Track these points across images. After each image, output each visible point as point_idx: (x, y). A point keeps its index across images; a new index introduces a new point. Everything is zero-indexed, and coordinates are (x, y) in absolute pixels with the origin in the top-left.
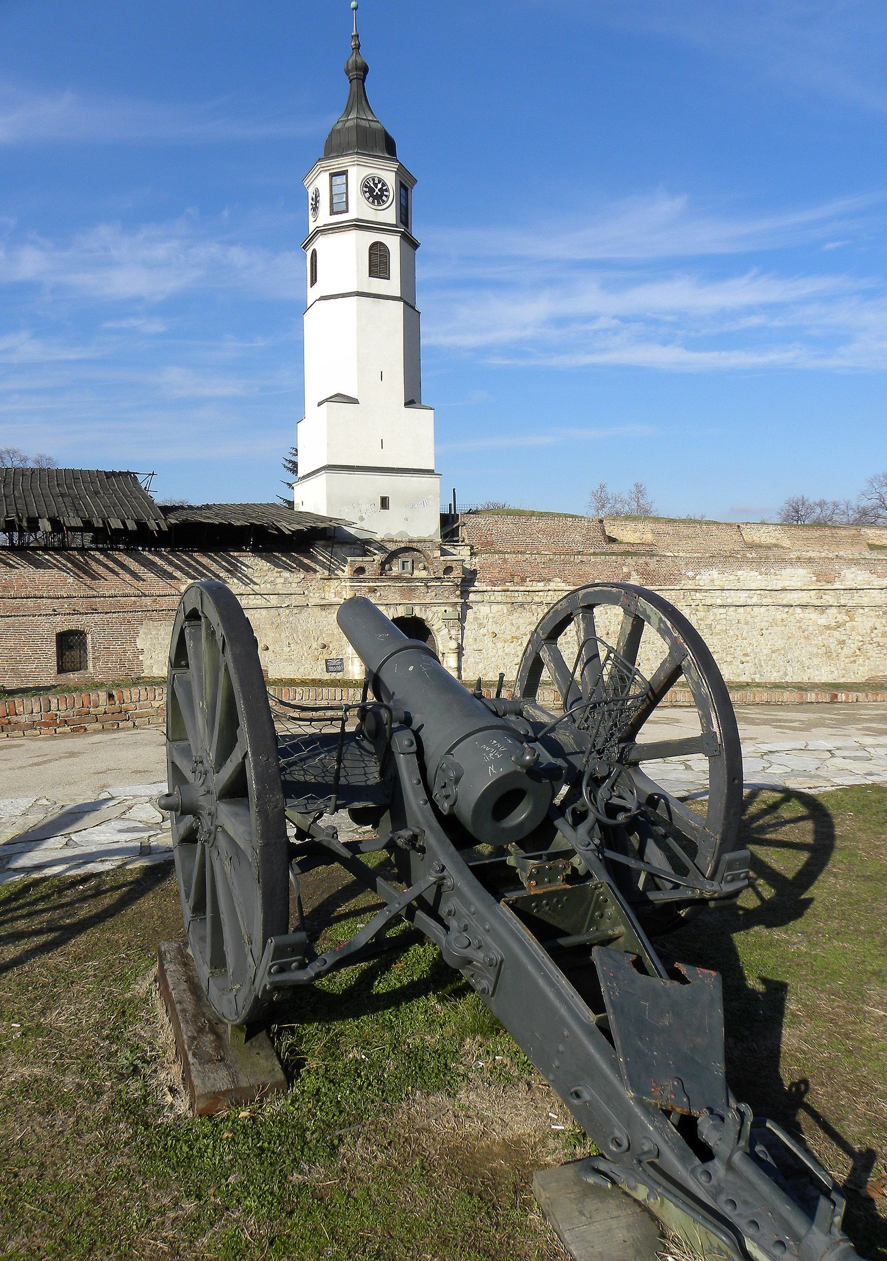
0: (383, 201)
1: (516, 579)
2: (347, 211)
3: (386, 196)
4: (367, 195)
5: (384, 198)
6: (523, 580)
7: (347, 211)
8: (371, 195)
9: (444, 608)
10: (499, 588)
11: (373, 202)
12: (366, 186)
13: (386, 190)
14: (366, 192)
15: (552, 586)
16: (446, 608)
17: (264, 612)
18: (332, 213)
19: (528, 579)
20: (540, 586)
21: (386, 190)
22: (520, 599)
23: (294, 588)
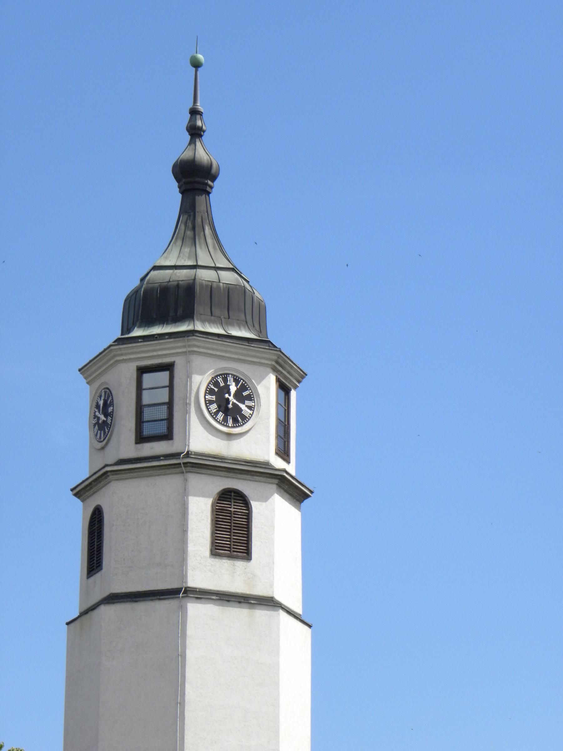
11: (225, 420)
14: (211, 402)
18: (141, 439)
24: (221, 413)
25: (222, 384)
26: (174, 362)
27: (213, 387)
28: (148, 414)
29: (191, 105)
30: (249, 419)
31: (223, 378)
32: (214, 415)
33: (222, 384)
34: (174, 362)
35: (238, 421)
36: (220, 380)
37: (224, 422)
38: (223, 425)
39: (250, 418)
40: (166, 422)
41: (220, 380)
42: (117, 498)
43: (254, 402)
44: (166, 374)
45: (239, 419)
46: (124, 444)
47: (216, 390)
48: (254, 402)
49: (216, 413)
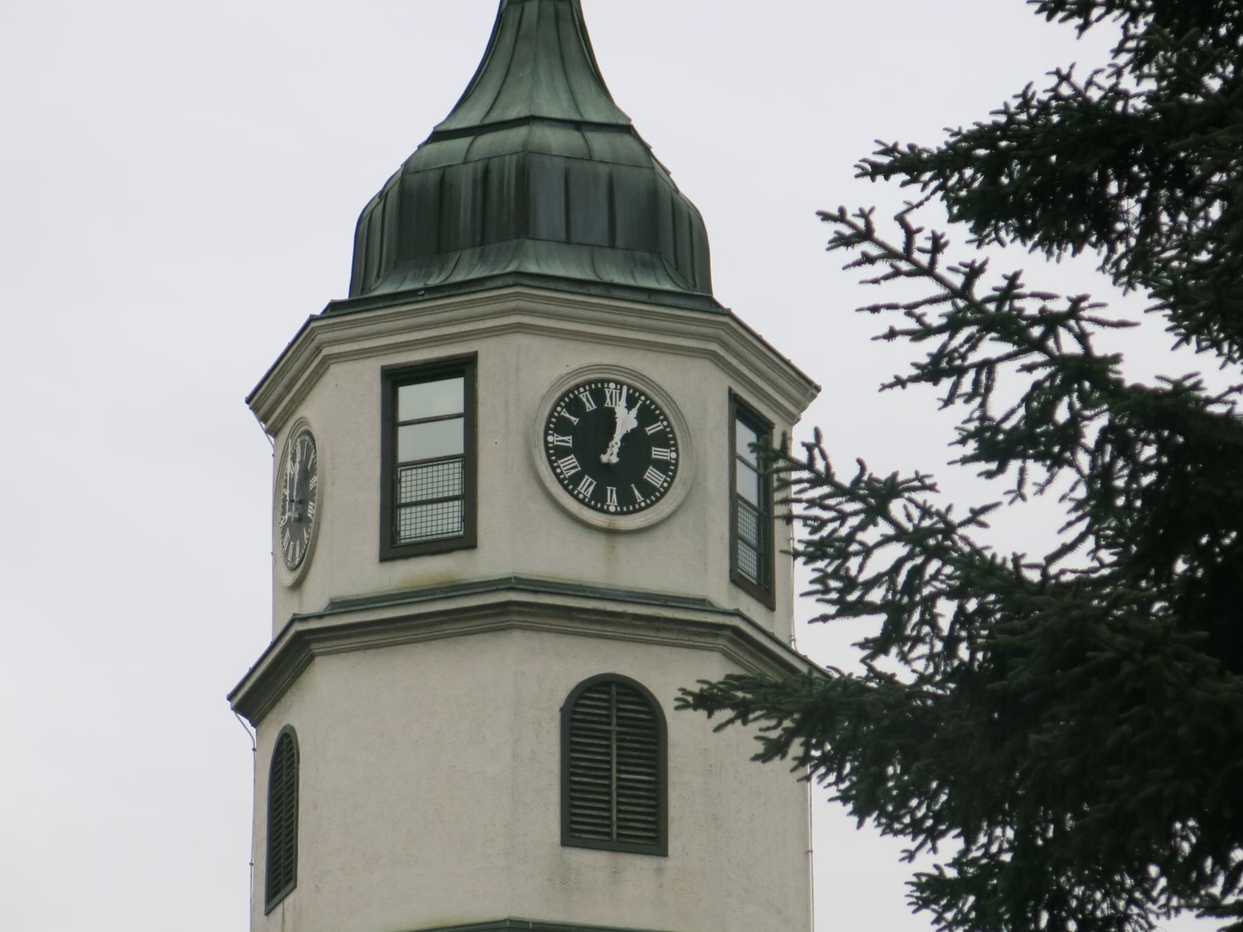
0: (648, 490)
2: (466, 541)
3: (663, 466)
4: (569, 465)
5: (653, 476)
7: (466, 541)
8: (591, 465)
12: (560, 426)
13: (664, 439)
14: (561, 452)
18: (393, 547)
21: (664, 439)
24: (587, 479)
25: (590, 406)
26: (476, 353)
27: (567, 415)
28: (411, 486)
30: (663, 495)
31: (592, 392)
33: (590, 406)
34: (476, 353)
35: (633, 500)
36: (585, 397)
37: (597, 501)
38: (594, 508)
39: (667, 490)
40: (403, 501)
41: (585, 397)
42: (331, 696)
43: (677, 451)
45: (637, 493)
46: (351, 564)
47: (575, 420)
48: (677, 451)
49: (576, 480)
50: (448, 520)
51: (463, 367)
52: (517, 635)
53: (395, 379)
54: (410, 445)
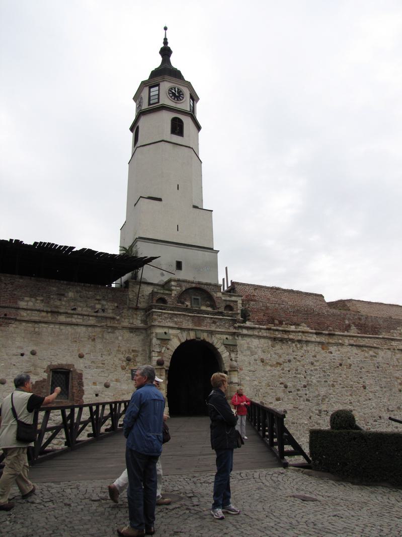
0: (180, 99)
1: (277, 322)
2: (158, 102)
6: (281, 323)
9: (225, 337)
10: (265, 327)
15: (300, 328)
16: (228, 336)
17: (84, 329)
18: (150, 104)
19: (284, 323)
20: (293, 328)
22: (279, 336)
23: (109, 313)
28: (152, 98)
29: (164, 37)
32: (171, 97)
44: (158, 87)
46: (145, 106)
50: (156, 101)
51: (158, 85)
52: (164, 111)
53: (150, 87)
54: (152, 94)
